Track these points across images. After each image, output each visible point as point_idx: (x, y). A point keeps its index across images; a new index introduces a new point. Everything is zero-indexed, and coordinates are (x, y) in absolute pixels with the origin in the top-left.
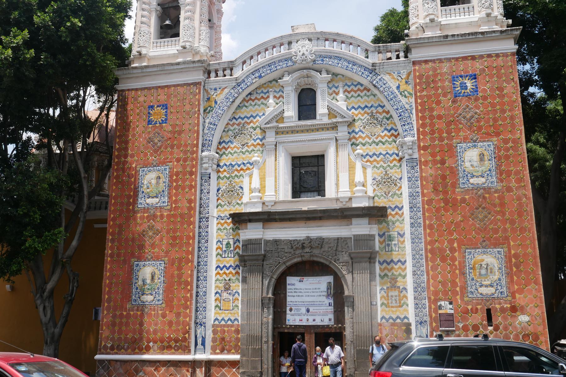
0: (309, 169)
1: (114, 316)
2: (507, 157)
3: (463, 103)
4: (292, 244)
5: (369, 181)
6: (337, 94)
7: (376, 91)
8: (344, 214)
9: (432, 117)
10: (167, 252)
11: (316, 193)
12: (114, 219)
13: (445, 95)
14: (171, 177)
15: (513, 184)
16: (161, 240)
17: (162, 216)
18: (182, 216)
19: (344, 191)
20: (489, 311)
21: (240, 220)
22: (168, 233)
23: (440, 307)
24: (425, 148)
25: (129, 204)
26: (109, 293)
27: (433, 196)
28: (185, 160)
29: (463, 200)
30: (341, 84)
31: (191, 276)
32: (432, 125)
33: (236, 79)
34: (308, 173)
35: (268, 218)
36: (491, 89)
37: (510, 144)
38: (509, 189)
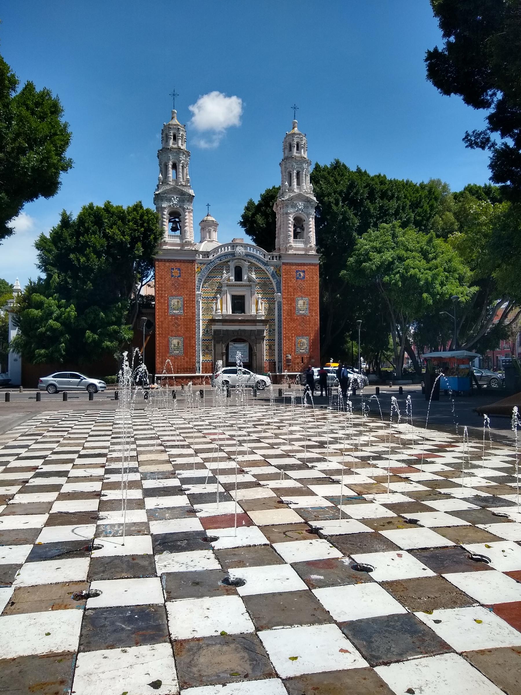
0: (238, 301)
1: (162, 359)
2: (313, 304)
3: (300, 282)
4: (234, 331)
5: (263, 309)
6: (252, 271)
7: (267, 272)
8: (254, 321)
9: (288, 286)
10: (184, 334)
11: (240, 312)
12: (158, 319)
13: (293, 278)
14: (184, 302)
15: (314, 314)
16: (181, 328)
17: (181, 319)
18: (190, 319)
19: (254, 312)
20: (302, 358)
21: (212, 321)
22: (184, 325)
23: (287, 357)
24: (285, 298)
25: (165, 312)
26: (159, 350)
27: (286, 317)
28: (190, 295)
29: (297, 319)
30: (253, 268)
31: (195, 343)
32: (288, 289)
33: (210, 260)
34: (239, 304)
35: (225, 321)
36: (309, 277)
37: (314, 299)
38: (312, 316)
